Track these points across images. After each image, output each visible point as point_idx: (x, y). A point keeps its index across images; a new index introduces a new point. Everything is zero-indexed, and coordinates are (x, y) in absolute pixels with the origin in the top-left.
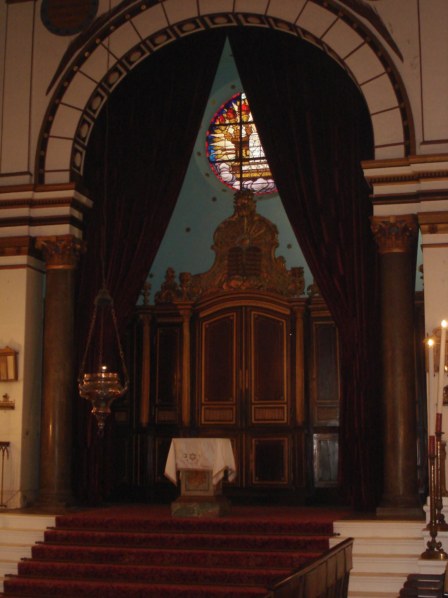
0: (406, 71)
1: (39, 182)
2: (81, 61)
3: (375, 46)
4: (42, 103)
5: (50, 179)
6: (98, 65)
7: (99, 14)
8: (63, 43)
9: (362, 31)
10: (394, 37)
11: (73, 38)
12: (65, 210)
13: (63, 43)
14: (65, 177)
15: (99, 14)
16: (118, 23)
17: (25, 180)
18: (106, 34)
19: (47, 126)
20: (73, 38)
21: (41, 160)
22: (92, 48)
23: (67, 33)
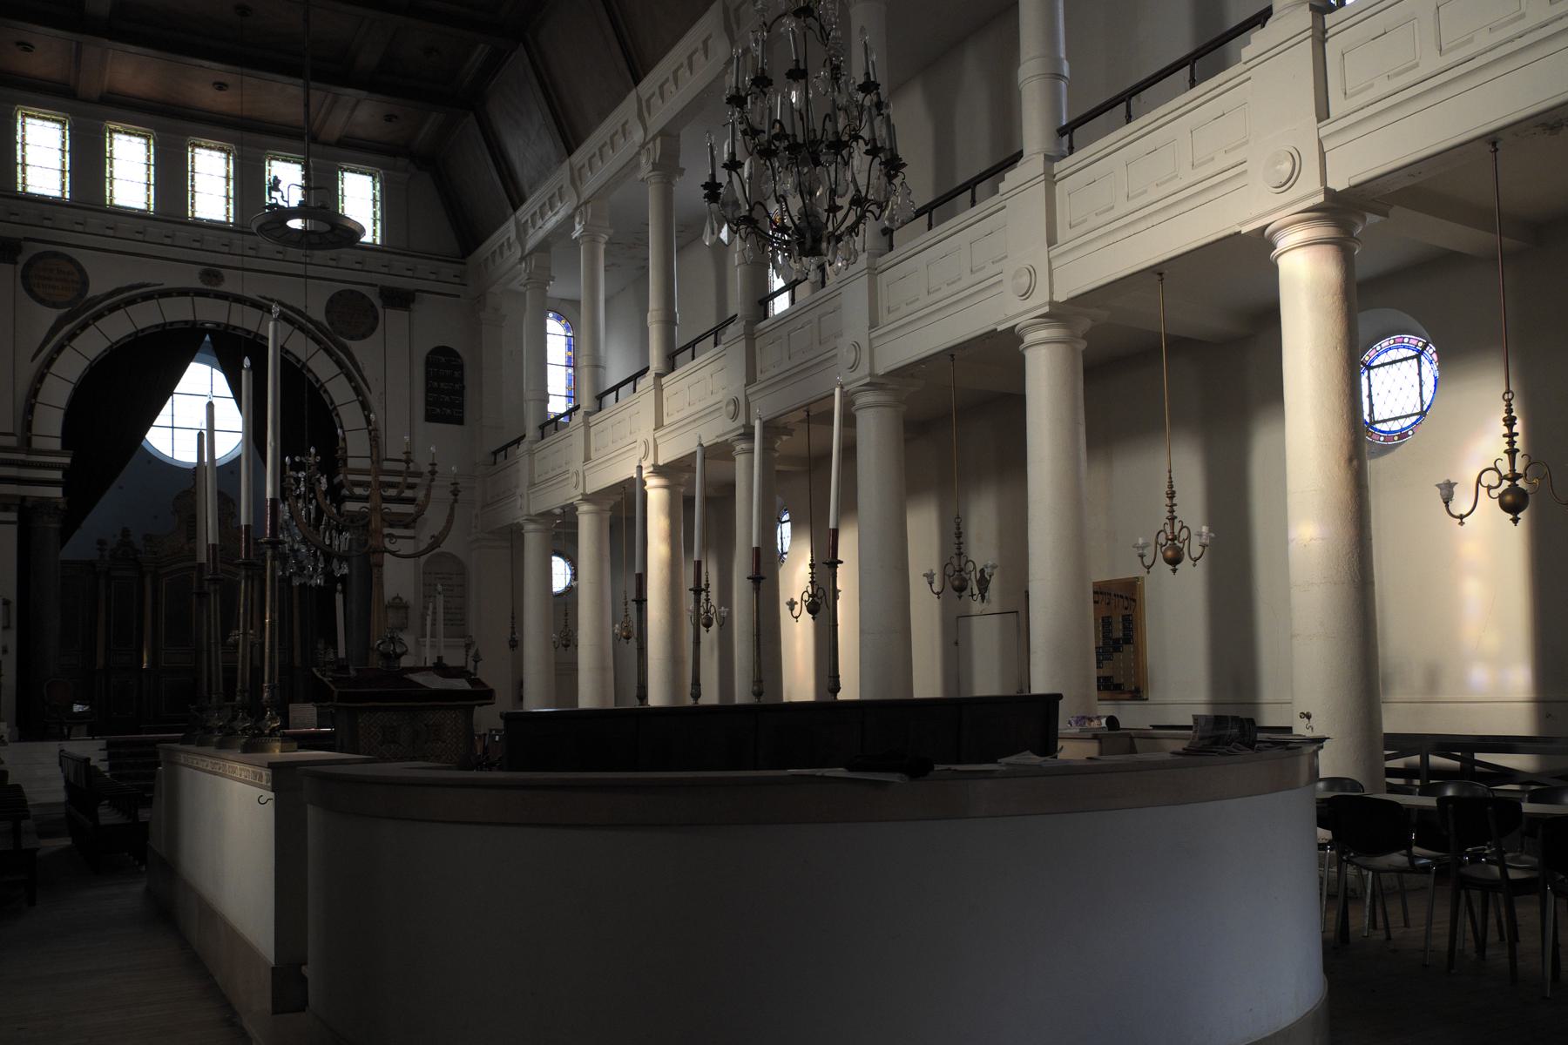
0: (373, 399)
1: (26, 444)
2: (72, 336)
3: (350, 378)
4: (29, 370)
5: (37, 443)
6: (93, 343)
7: (90, 295)
8: (50, 316)
9: (339, 363)
10: (365, 374)
11: (62, 311)
12: (58, 475)
13: (50, 316)
14: (56, 444)
15: (90, 295)
16: (112, 309)
17: (12, 441)
18: (99, 316)
19: (34, 392)
20: (62, 311)
21: (28, 426)
22: (84, 326)
23: (54, 305)
